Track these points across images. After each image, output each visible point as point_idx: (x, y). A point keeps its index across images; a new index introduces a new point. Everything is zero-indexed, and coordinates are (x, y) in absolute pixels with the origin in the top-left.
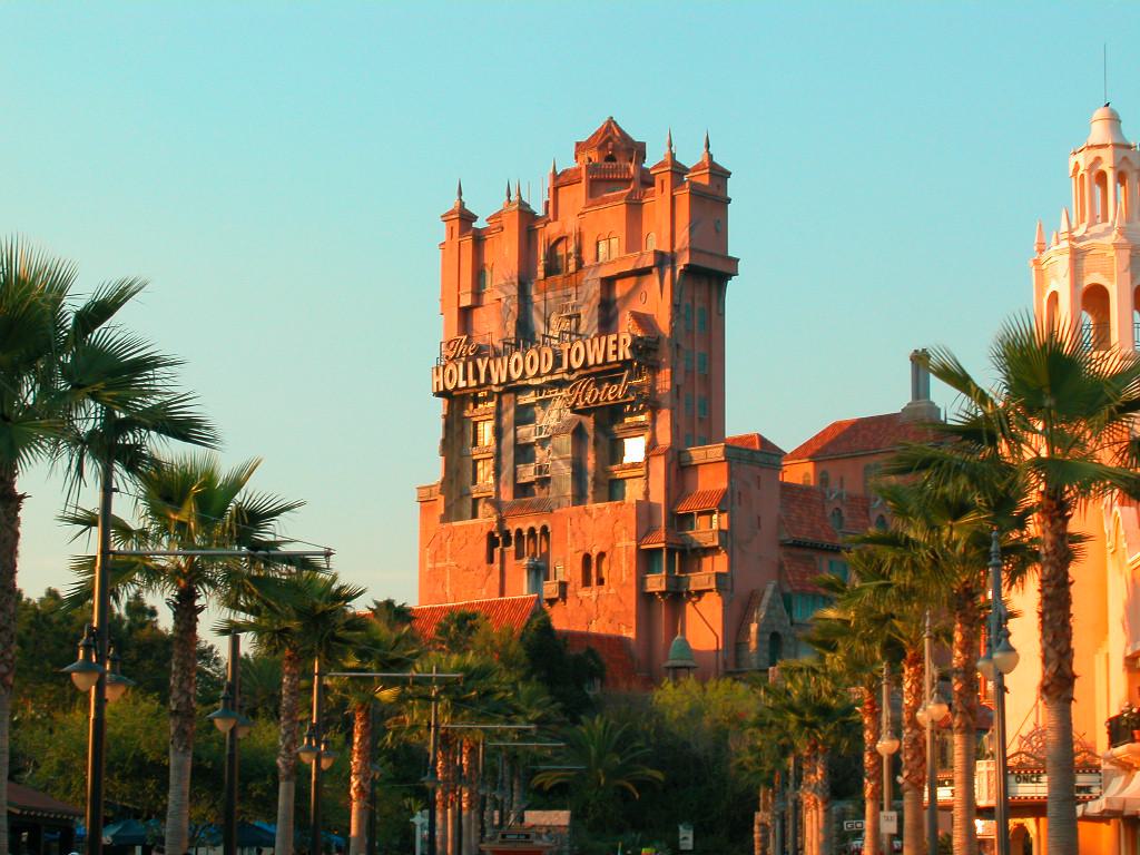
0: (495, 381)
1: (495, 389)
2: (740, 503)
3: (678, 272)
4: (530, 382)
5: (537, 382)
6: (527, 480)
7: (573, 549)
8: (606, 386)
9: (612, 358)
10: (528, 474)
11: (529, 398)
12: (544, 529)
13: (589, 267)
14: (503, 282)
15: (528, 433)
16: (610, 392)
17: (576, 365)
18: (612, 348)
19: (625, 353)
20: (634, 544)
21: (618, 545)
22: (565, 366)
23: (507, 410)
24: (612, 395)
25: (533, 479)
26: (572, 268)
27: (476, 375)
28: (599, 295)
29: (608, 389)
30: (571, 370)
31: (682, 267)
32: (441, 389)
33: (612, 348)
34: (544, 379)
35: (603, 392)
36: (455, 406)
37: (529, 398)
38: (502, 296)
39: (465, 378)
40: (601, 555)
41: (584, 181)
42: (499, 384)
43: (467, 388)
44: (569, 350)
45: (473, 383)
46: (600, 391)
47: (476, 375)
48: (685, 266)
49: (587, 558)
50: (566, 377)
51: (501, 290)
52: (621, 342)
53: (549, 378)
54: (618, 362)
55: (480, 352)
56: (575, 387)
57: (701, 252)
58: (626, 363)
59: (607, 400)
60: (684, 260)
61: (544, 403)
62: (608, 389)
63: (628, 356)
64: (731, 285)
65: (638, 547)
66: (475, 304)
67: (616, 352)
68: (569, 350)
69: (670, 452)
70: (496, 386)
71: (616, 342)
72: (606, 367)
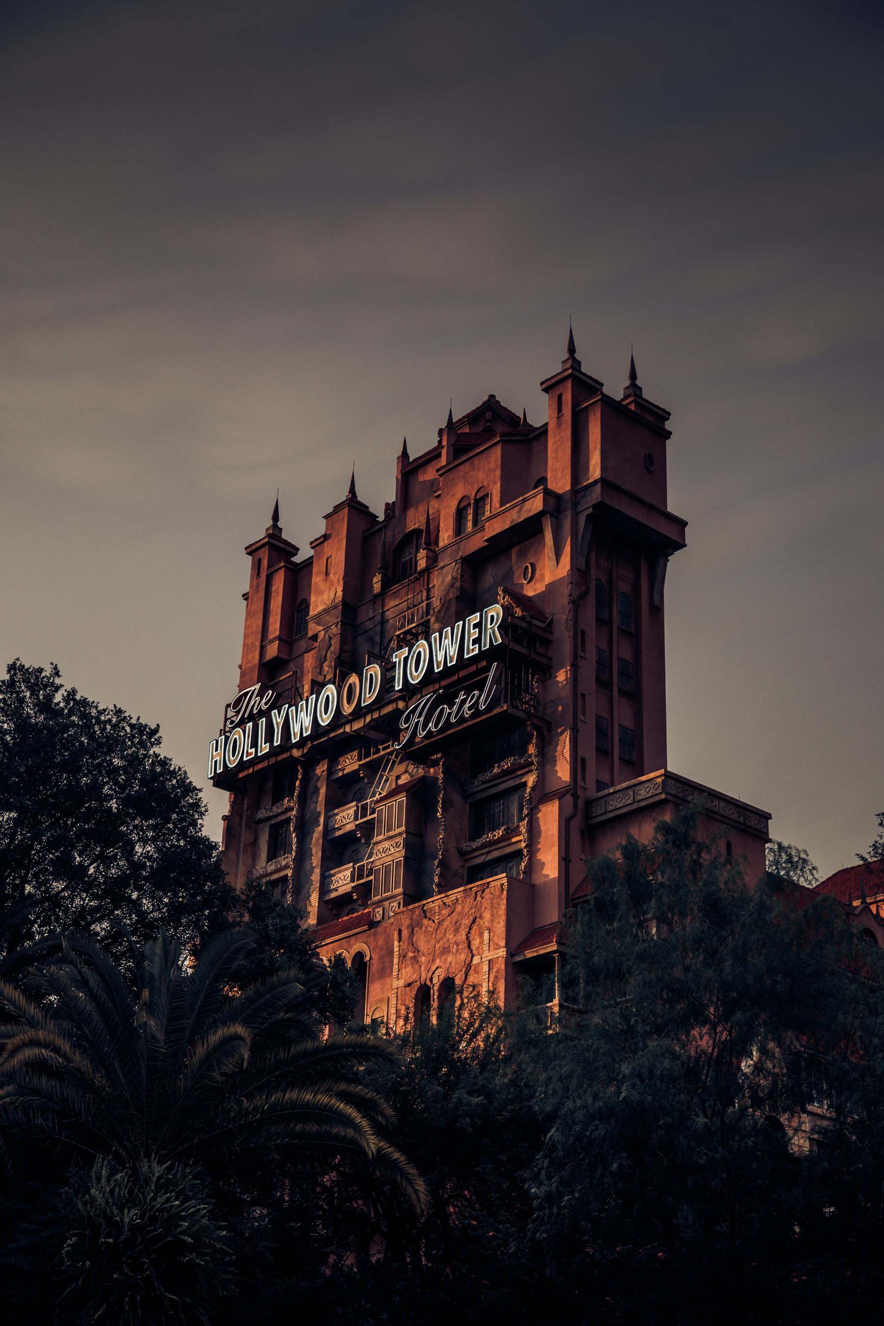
1: (296, 753)
3: (582, 520)
5: (358, 725)
6: (341, 891)
8: (462, 697)
11: (350, 763)
12: (359, 956)
13: (446, 548)
16: (467, 705)
17: (416, 677)
20: (502, 952)
21: (476, 960)
22: (398, 687)
24: (470, 708)
25: (348, 888)
26: (422, 564)
27: (270, 738)
28: (458, 584)
29: (463, 702)
30: (410, 691)
31: (590, 510)
35: (455, 708)
36: (246, 802)
37: (350, 763)
39: (254, 744)
40: (448, 985)
41: (444, 452)
42: (303, 741)
43: (257, 760)
44: (406, 659)
46: (451, 707)
47: (270, 738)
48: (595, 506)
50: (401, 705)
60: (596, 495)
61: (373, 769)
62: (463, 702)
64: (676, 563)
65: (510, 954)
66: (285, 657)
69: (568, 799)
71: (478, 625)
72: (462, 673)
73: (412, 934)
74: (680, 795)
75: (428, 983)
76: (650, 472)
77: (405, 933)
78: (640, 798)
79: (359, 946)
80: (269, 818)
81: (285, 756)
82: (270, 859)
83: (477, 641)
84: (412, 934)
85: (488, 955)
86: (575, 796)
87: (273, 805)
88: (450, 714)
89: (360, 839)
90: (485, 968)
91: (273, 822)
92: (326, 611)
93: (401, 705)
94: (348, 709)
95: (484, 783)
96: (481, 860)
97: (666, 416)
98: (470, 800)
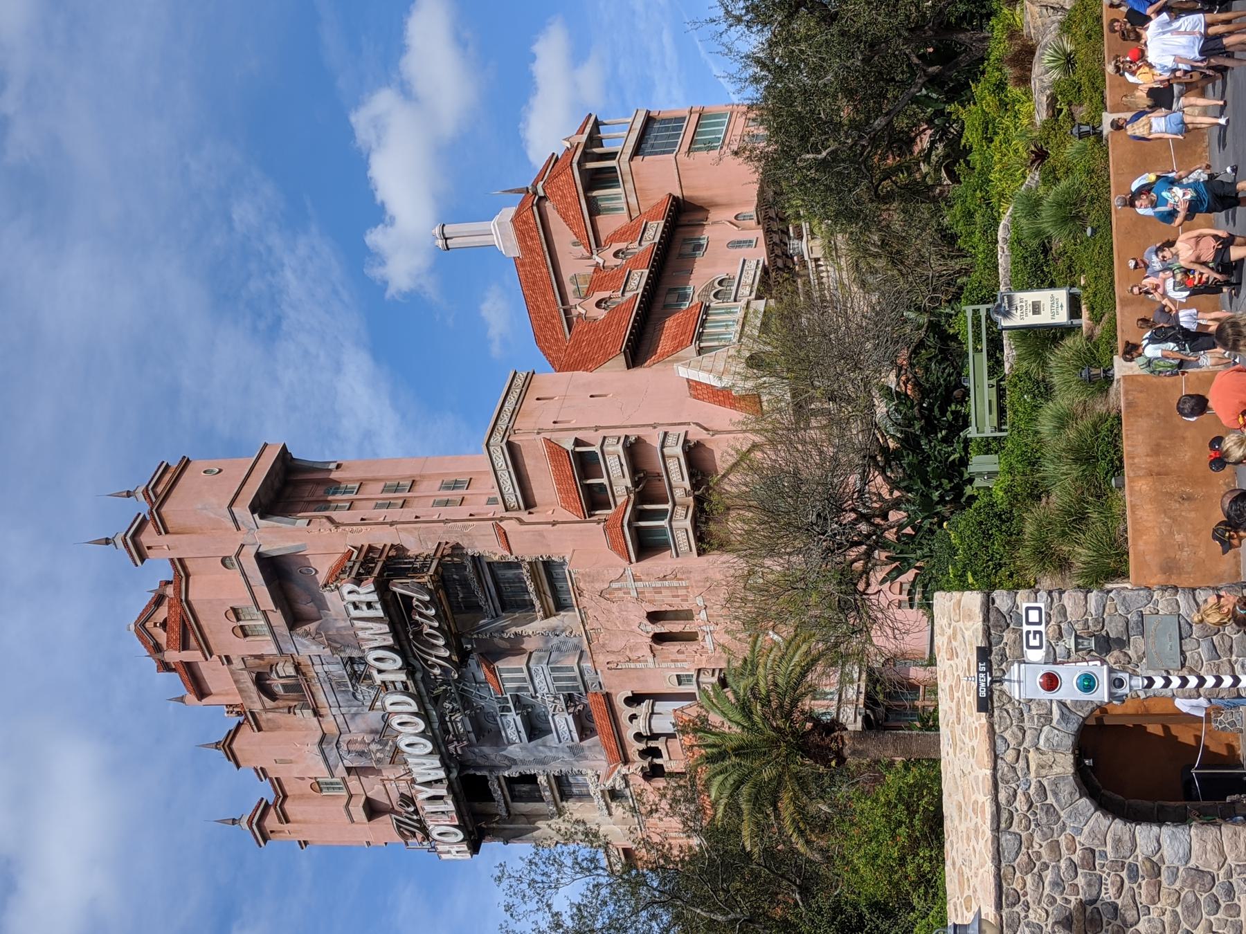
0: (442, 774)
1: (454, 774)
2: (569, 422)
4: (436, 725)
6: (573, 727)
7: (650, 659)
8: (417, 617)
9: (380, 613)
10: (563, 722)
14: (323, 766)
15: (513, 723)
16: (424, 611)
18: (366, 613)
19: (367, 592)
22: (403, 677)
23: (485, 756)
25: (570, 718)
29: (421, 615)
30: (409, 668)
31: (256, 516)
32: (464, 847)
33: (366, 613)
34: (429, 707)
38: (341, 767)
44: (380, 671)
45: (450, 806)
49: (659, 638)
50: (419, 676)
51: (337, 766)
52: (354, 598)
53: (426, 699)
54: (383, 600)
55: (408, 800)
56: (426, 661)
57: (237, 494)
58: (382, 588)
59: (436, 616)
62: (421, 615)
63: (372, 588)
67: (369, 605)
68: (380, 671)
70: (448, 771)
71: (356, 607)
73: (613, 652)
74: (502, 433)
75: (651, 635)
76: (220, 471)
77: (611, 658)
78: (504, 465)
79: (619, 702)
80: (506, 803)
81: (455, 785)
82: (541, 799)
83: (369, 605)
84: (613, 652)
85: (630, 583)
86: (502, 519)
87: (494, 801)
88: (431, 627)
89: (528, 713)
90: (639, 584)
91: (509, 799)
92: (326, 760)
93: (419, 676)
94: (421, 725)
95: (487, 600)
96: (550, 600)
97: (164, 465)
98: (500, 612)
